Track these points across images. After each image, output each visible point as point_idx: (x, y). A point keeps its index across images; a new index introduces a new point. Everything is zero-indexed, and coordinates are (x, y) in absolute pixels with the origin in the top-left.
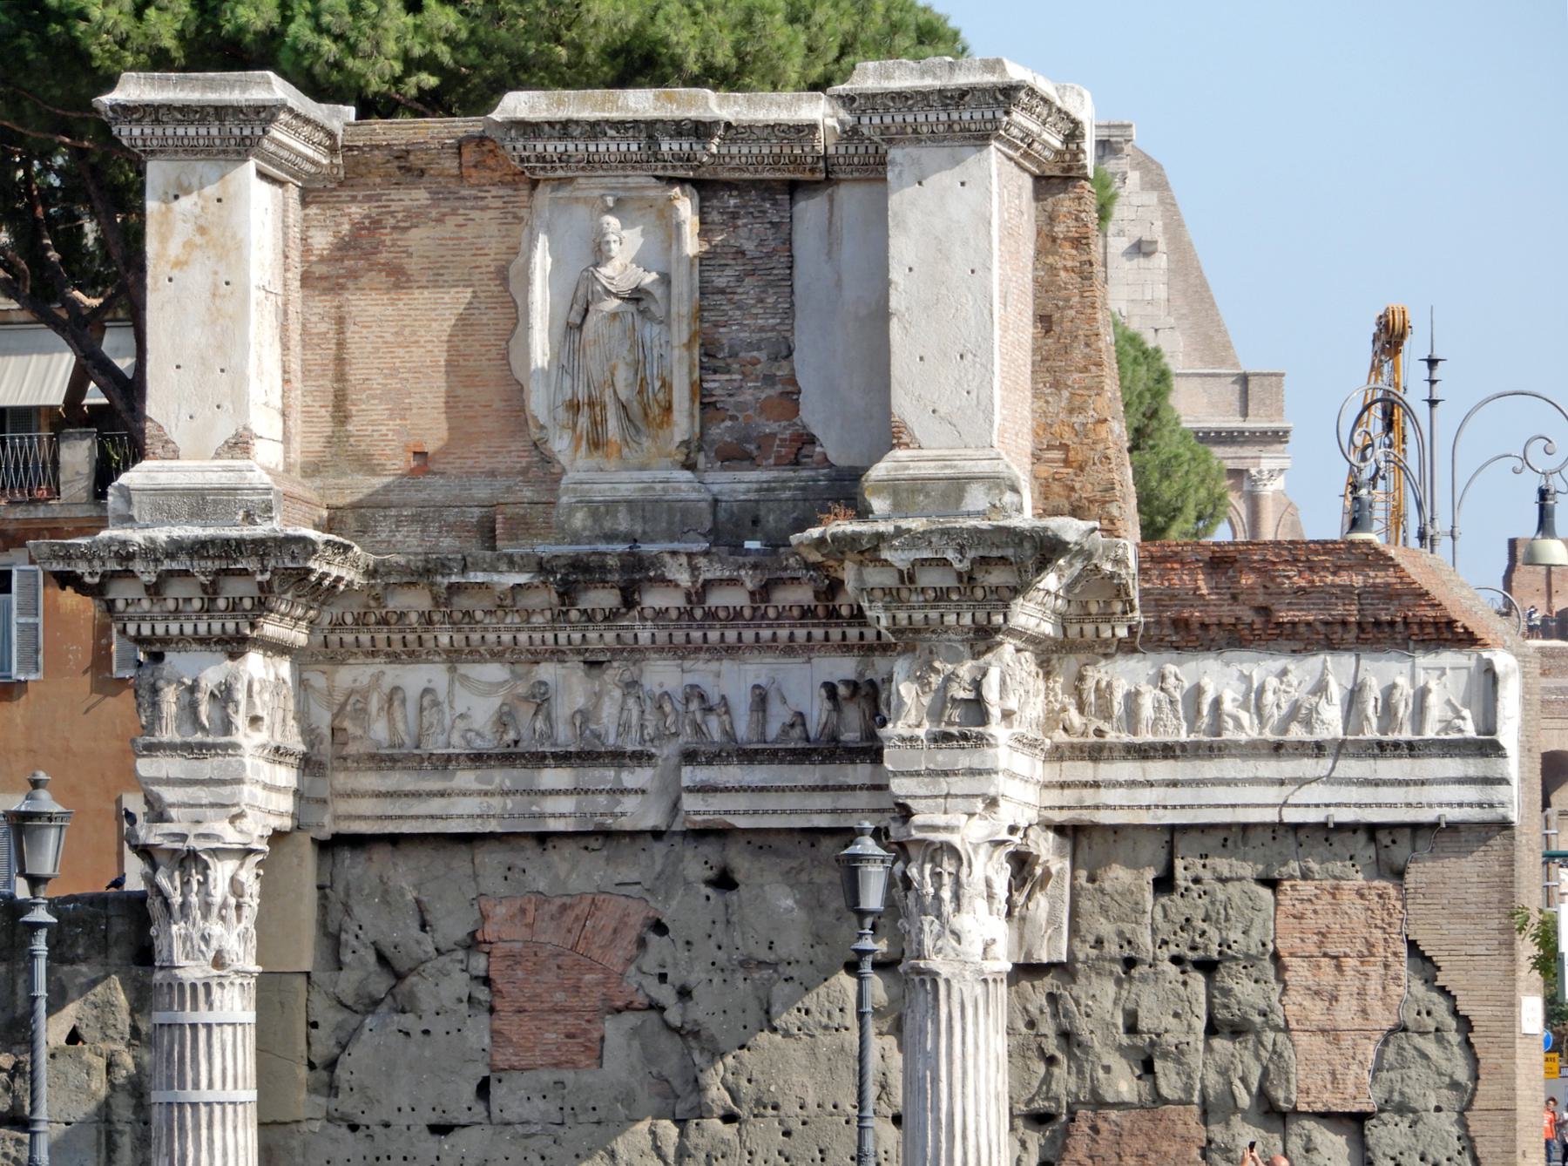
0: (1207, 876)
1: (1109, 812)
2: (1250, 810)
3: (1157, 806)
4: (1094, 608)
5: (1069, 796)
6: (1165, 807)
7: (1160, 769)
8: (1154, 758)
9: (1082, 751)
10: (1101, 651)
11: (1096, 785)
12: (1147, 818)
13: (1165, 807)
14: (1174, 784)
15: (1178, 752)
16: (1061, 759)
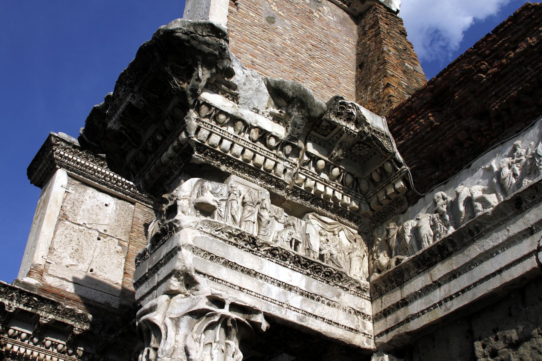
0: (500, 345)
1: (416, 320)
2: (513, 269)
3: (446, 300)
4: (376, 177)
5: (390, 320)
6: (451, 298)
7: (440, 270)
8: (435, 263)
9: (392, 282)
10: (398, 210)
11: (404, 303)
12: (440, 313)
13: (451, 298)
14: (453, 275)
15: (450, 249)
16: (381, 295)
